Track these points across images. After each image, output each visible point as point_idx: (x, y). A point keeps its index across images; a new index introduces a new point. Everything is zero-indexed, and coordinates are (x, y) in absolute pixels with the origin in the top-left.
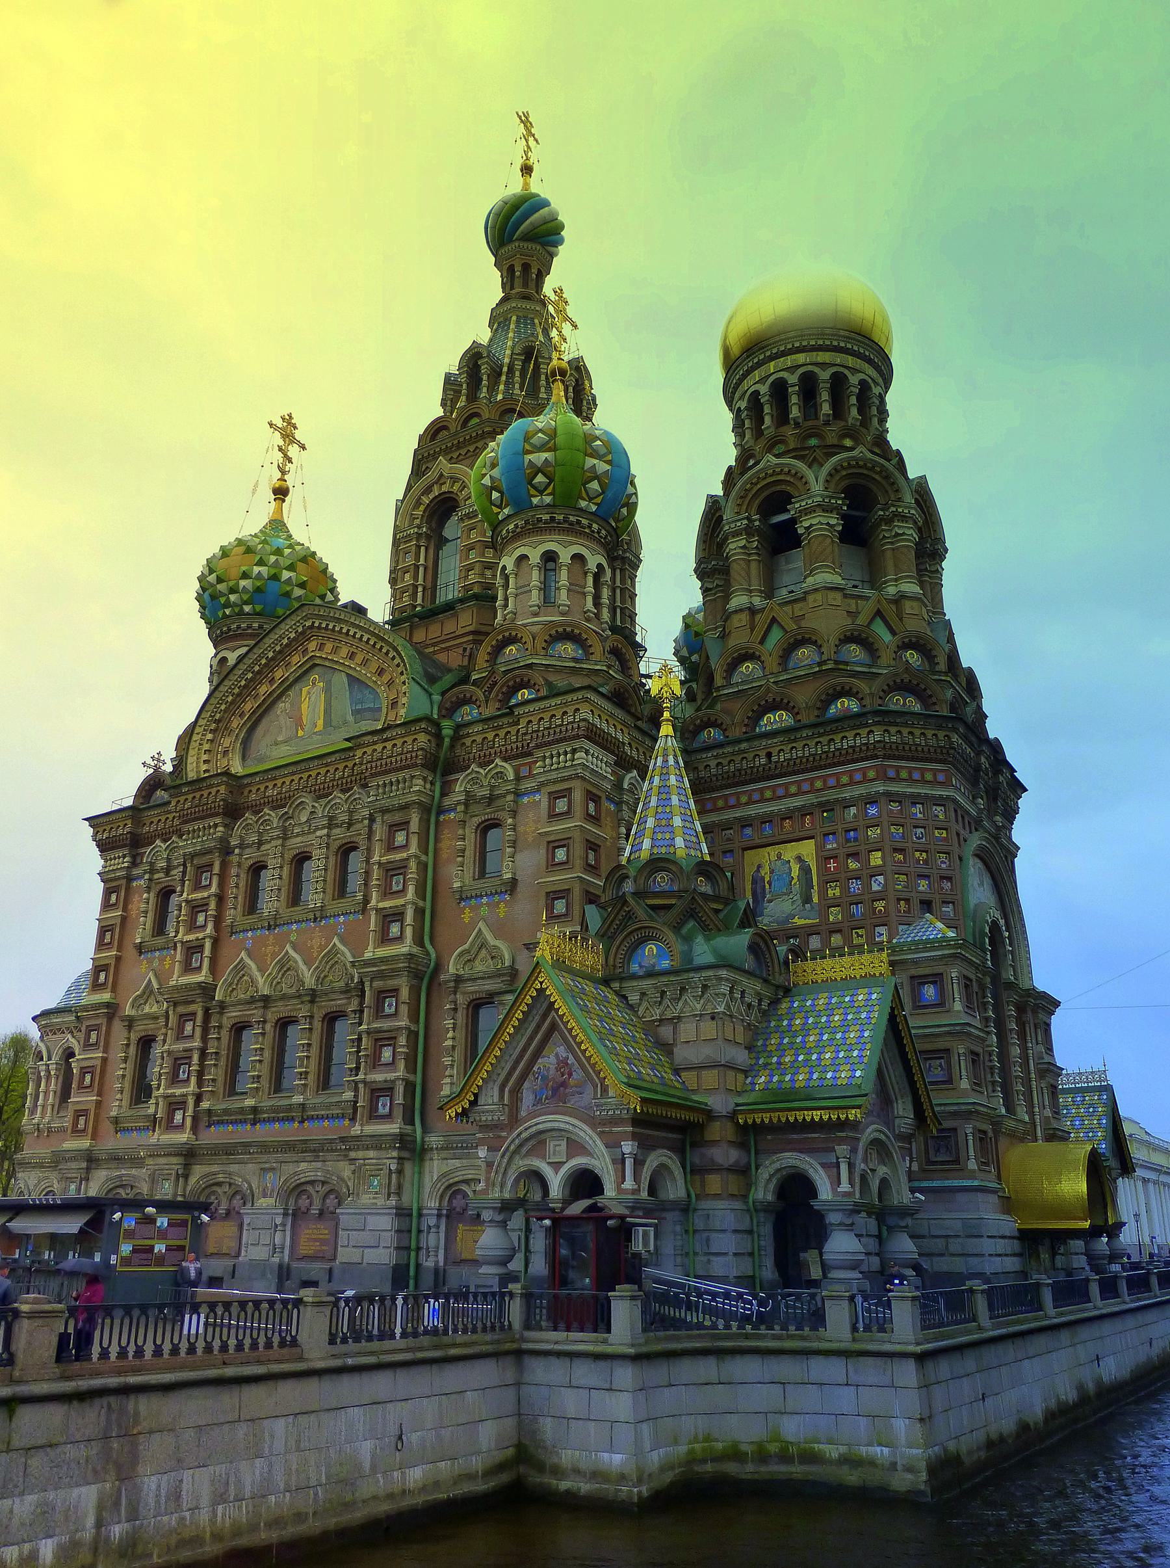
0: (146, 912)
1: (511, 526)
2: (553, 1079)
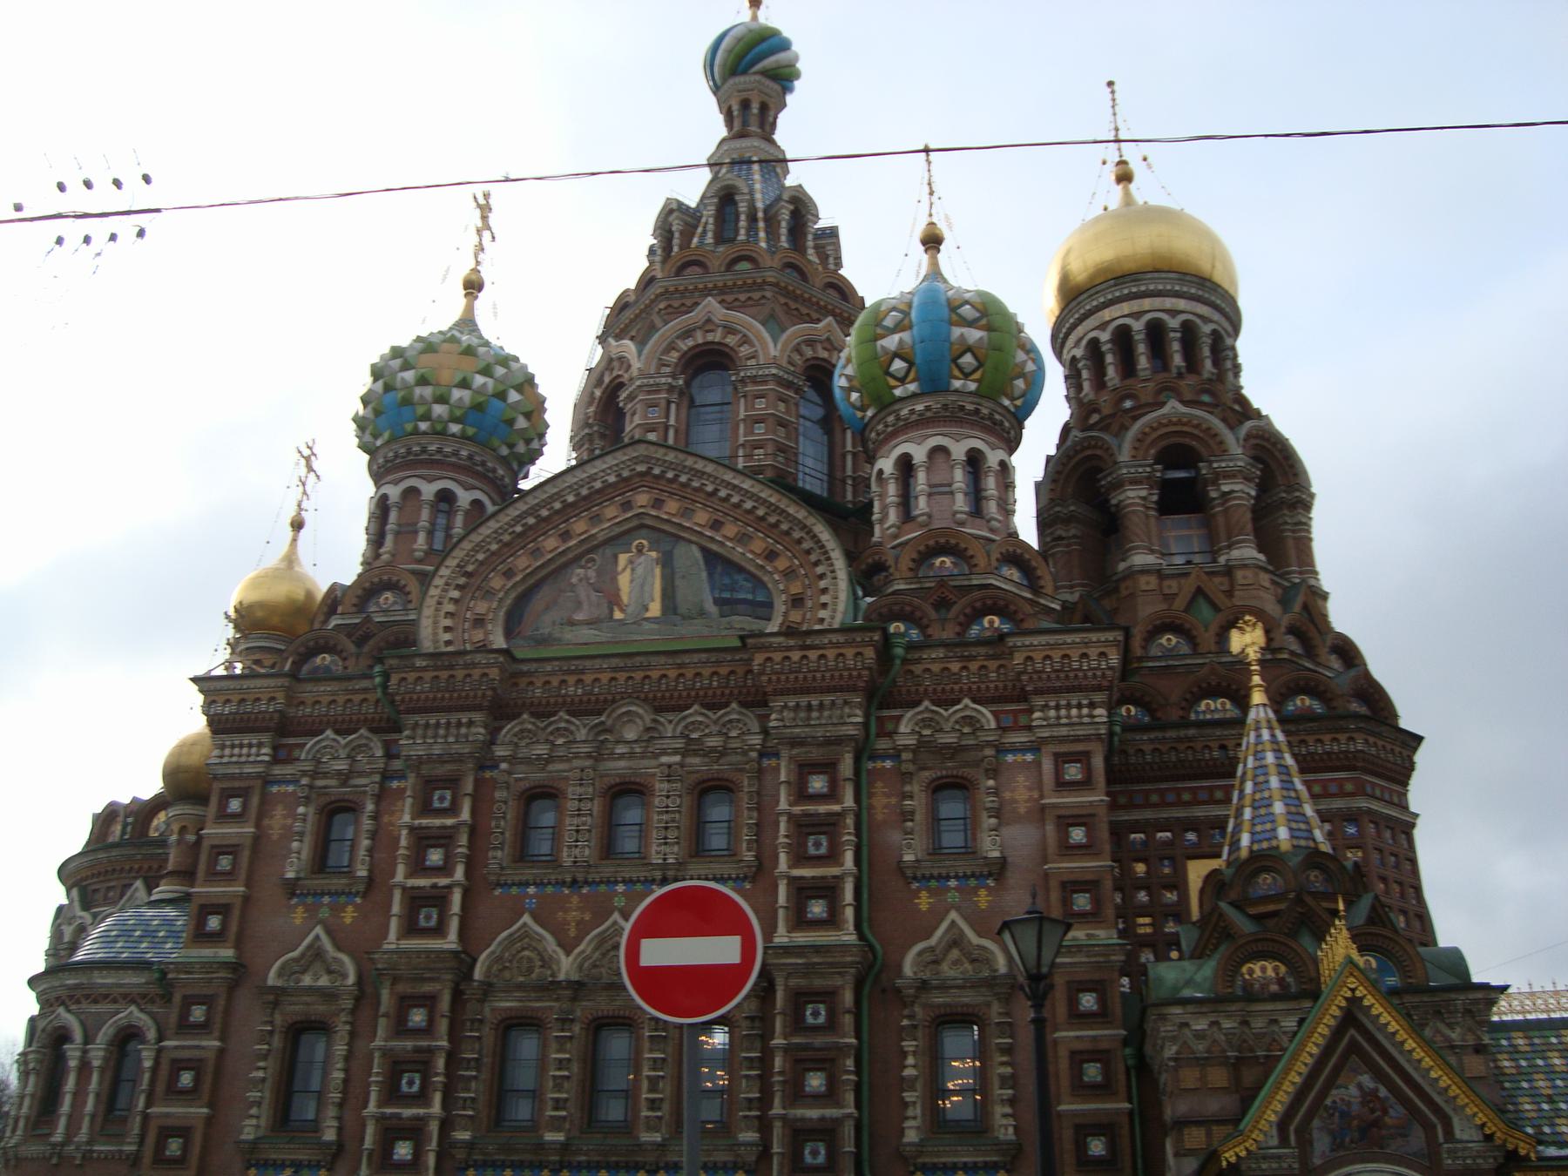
0: (301, 834)
1: (920, 407)
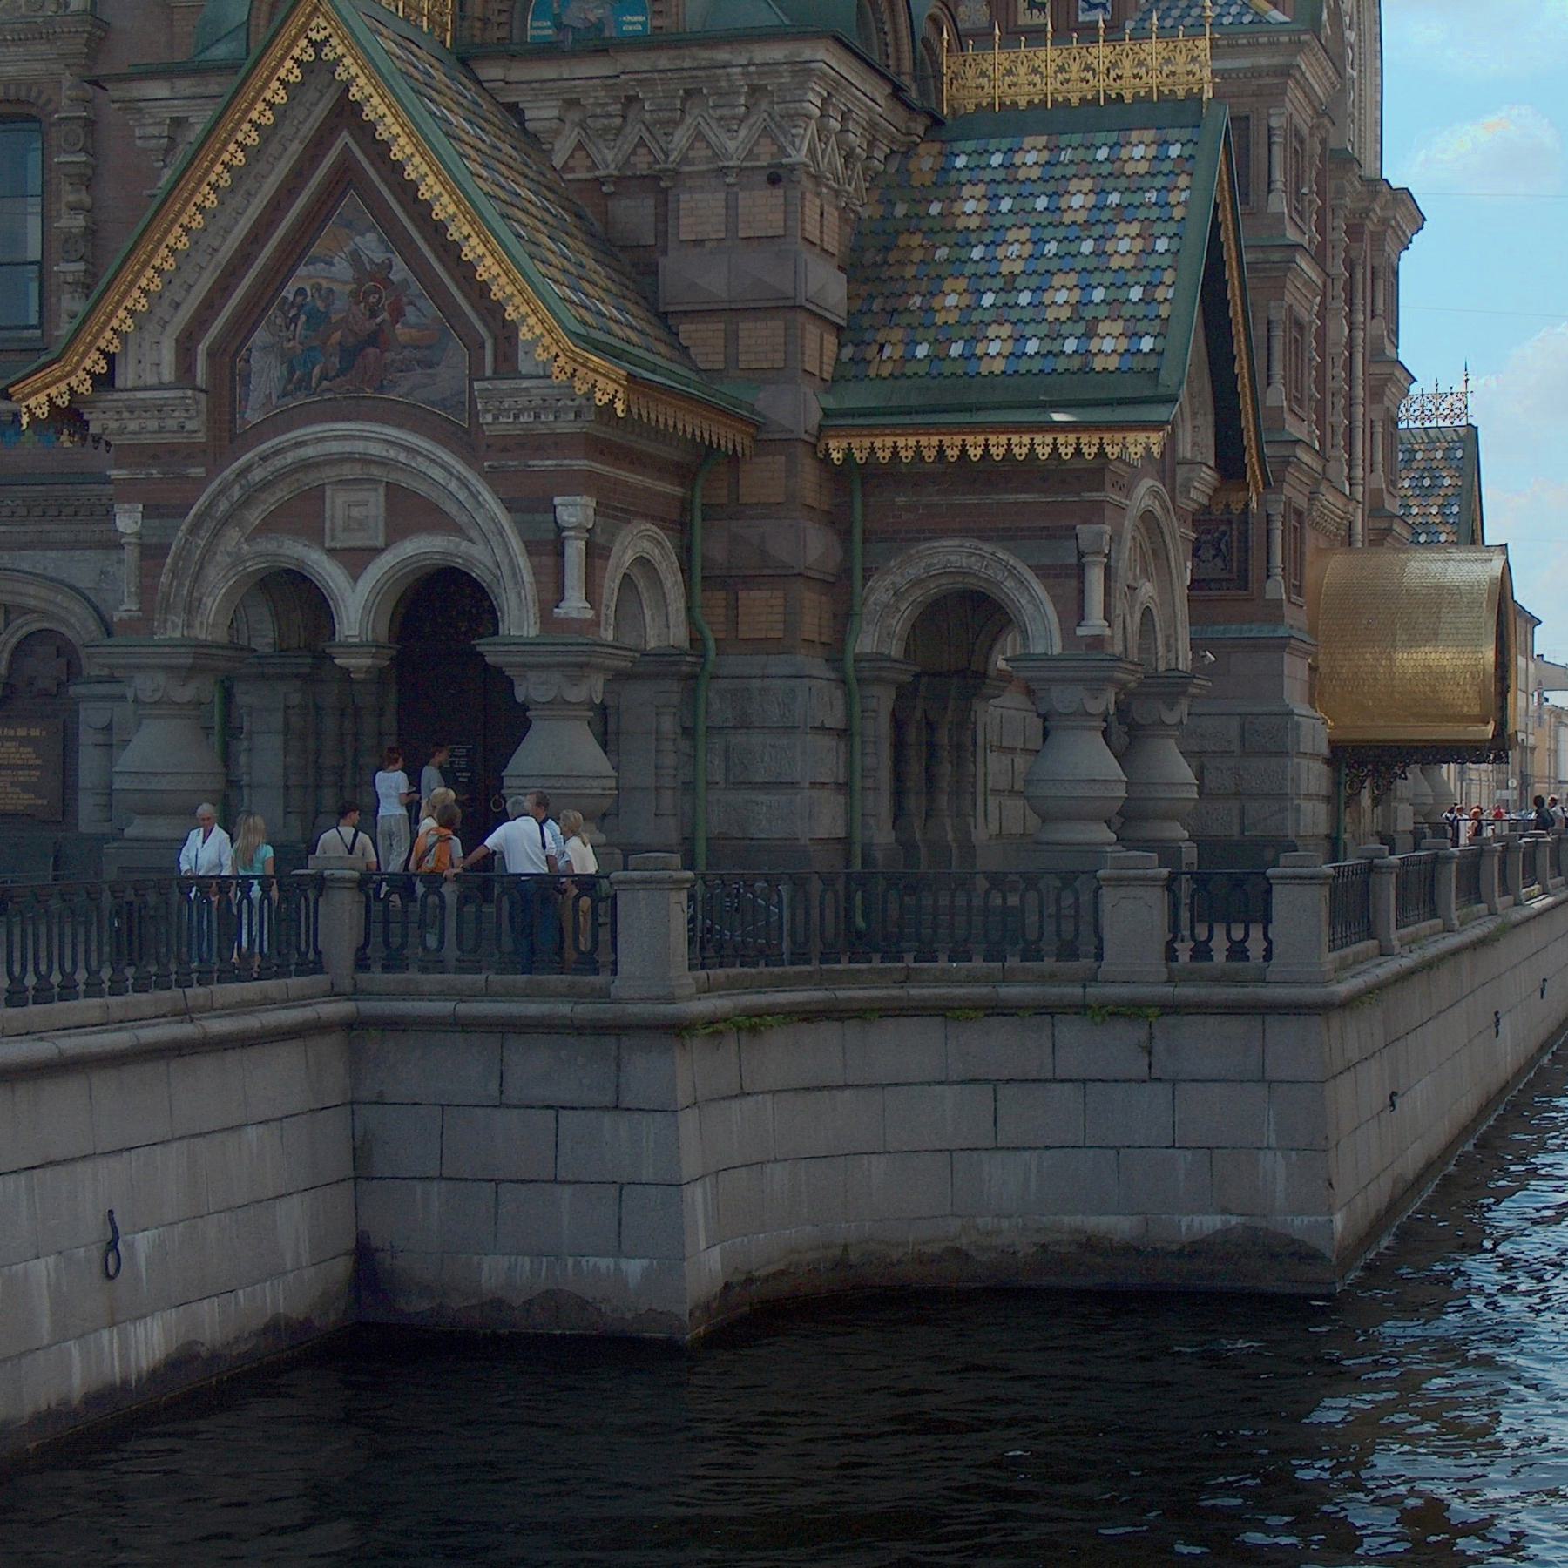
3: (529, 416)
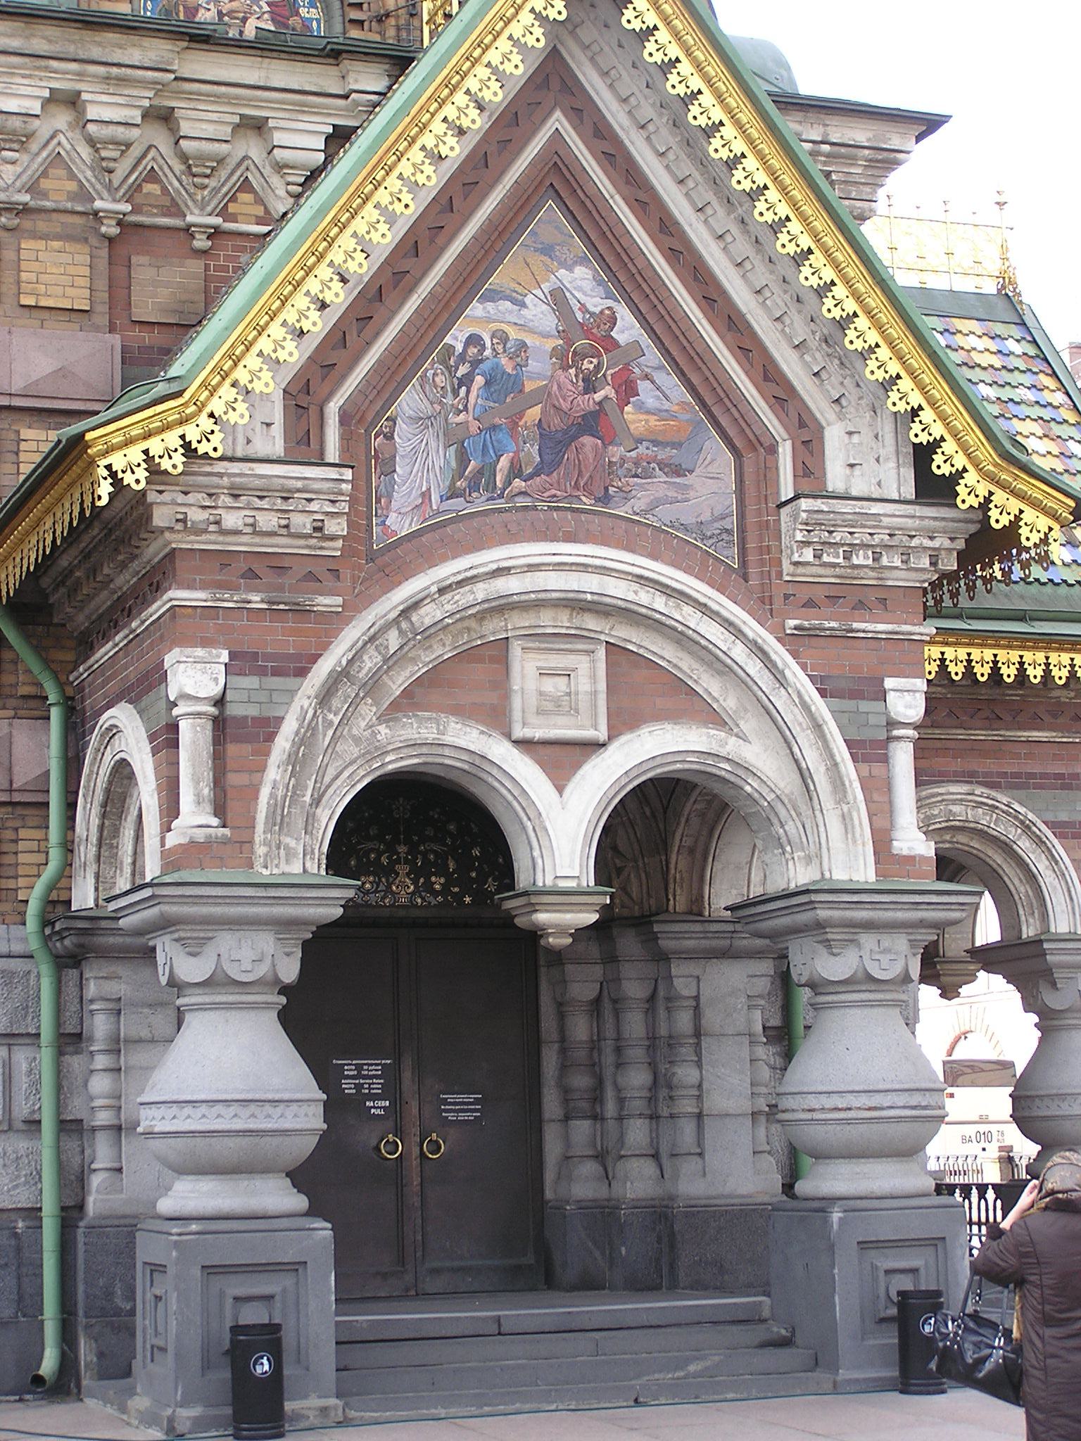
2: (543, 395)
3: (866, 557)
